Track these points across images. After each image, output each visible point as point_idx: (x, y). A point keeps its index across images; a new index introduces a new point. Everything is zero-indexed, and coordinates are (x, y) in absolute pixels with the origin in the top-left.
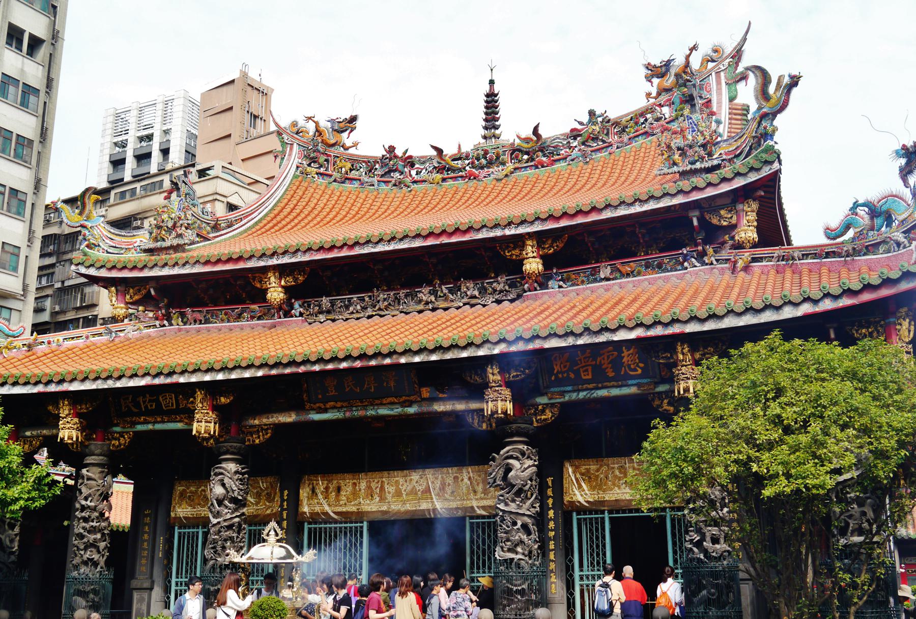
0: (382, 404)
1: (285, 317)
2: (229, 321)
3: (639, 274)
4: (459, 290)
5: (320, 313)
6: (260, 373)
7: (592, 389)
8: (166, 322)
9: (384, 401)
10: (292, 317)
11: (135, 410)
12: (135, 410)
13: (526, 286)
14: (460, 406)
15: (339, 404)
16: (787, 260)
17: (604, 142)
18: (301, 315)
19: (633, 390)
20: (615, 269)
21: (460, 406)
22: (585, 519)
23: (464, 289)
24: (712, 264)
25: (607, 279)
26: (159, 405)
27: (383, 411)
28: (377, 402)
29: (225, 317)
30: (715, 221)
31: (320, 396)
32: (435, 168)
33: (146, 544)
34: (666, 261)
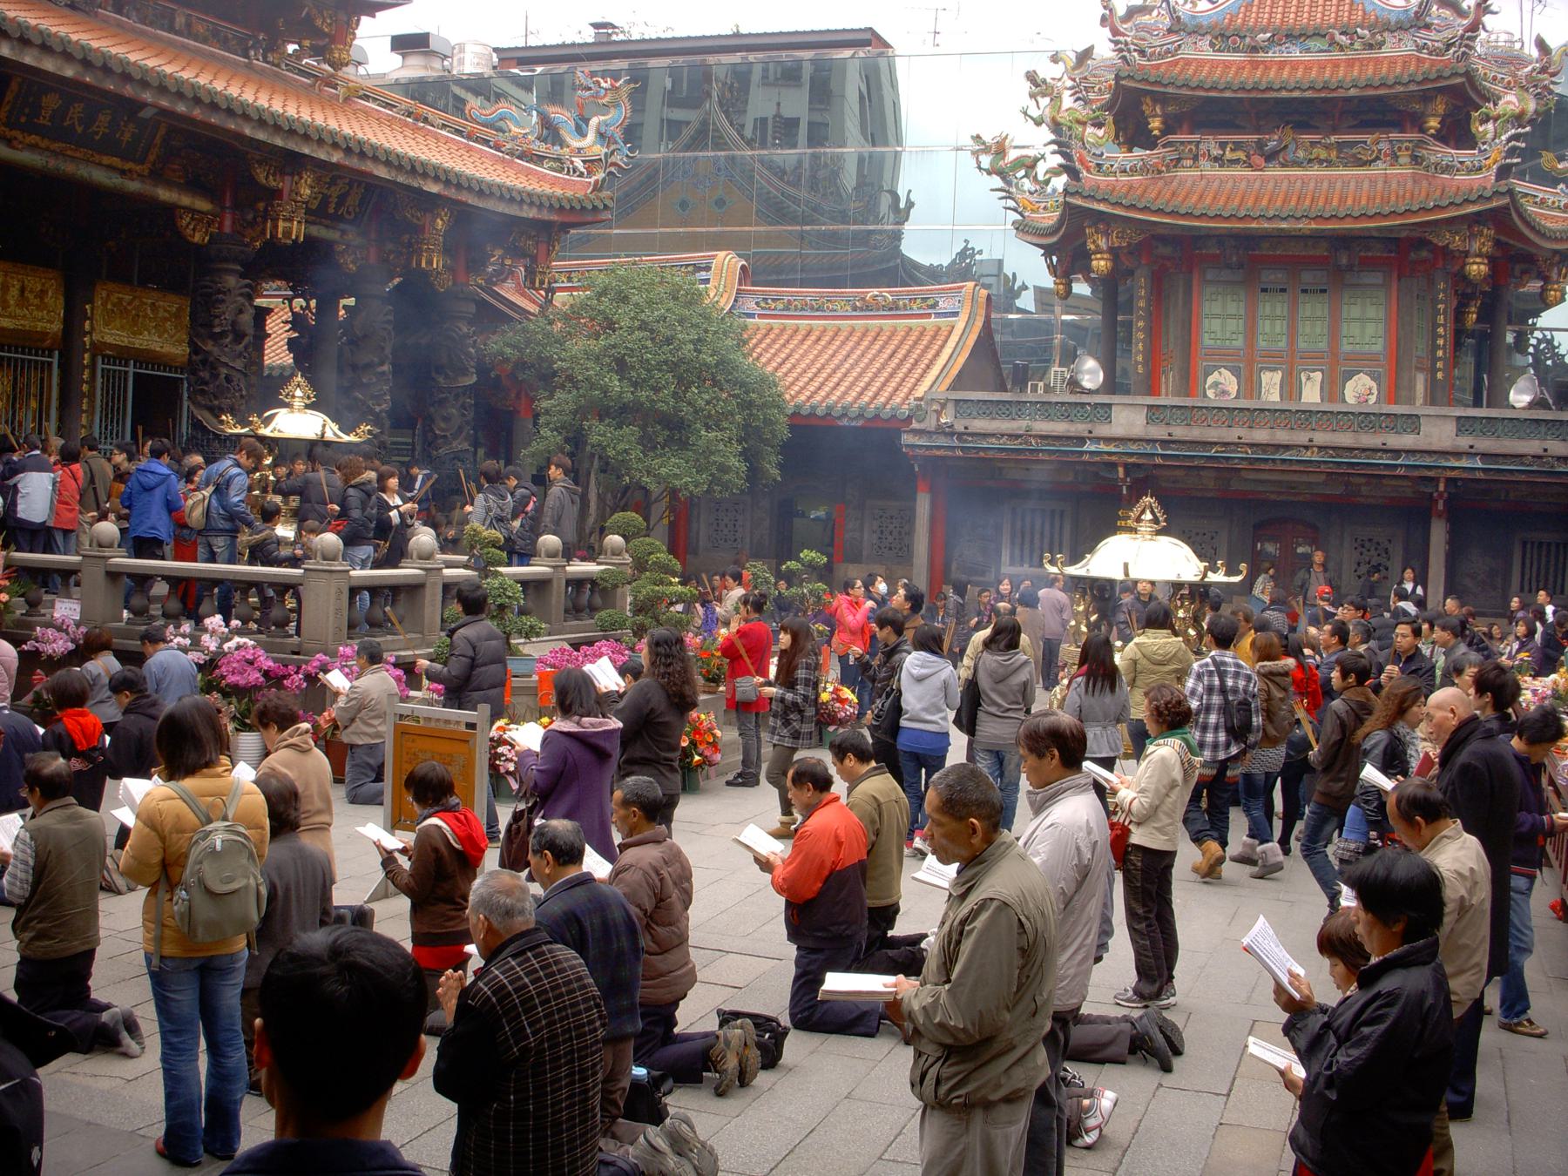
0: (100, 164)
3: (205, 41)
6: (69, 72)
9: (106, 160)
14: (186, 200)
15: (44, 143)
16: (417, 119)
20: (189, 25)
21: (186, 200)
22: (23, 360)
24: (278, 66)
25: (176, 33)
27: (100, 176)
28: (97, 158)
30: (319, 22)
31: (23, 120)
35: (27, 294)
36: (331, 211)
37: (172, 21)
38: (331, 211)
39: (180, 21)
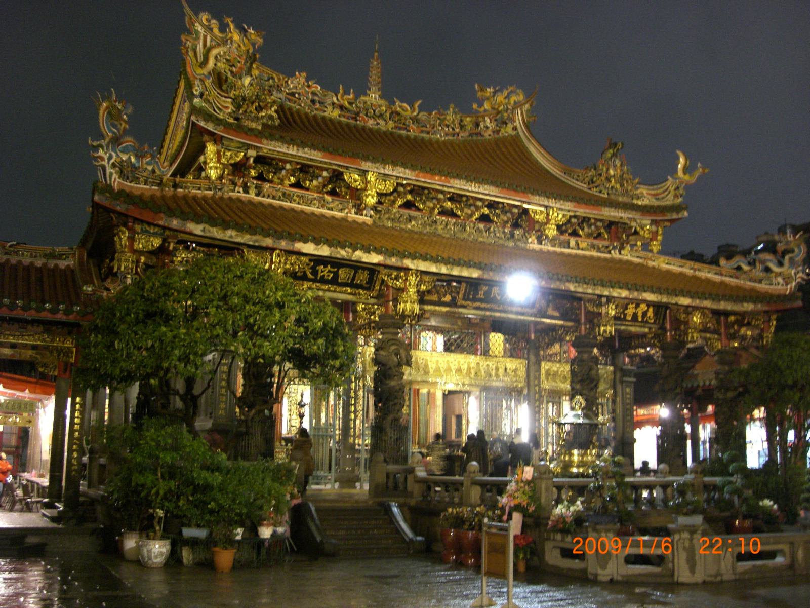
1: (356, 213)
2: (299, 203)
4: (489, 229)
5: (389, 219)
7: (627, 325)
8: (241, 190)
10: (362, 215)
11: (310, 276)
12: (310, 276)
13: (530, 240)
17: (453, 129)
18: (371, 217)
19: (647, 330)
23: (492, 229)
25: (572, 249)
26: (336, 275)
29: (297, 199)
30: (642, 233)
31: (471, 297)
32: (333, 104)
33: (224, 390)
34: (601, 246)
35: (508, 371)
36: (640, 319)
37: (569, 243)
38: (640, 319)
39: (572, 242)
